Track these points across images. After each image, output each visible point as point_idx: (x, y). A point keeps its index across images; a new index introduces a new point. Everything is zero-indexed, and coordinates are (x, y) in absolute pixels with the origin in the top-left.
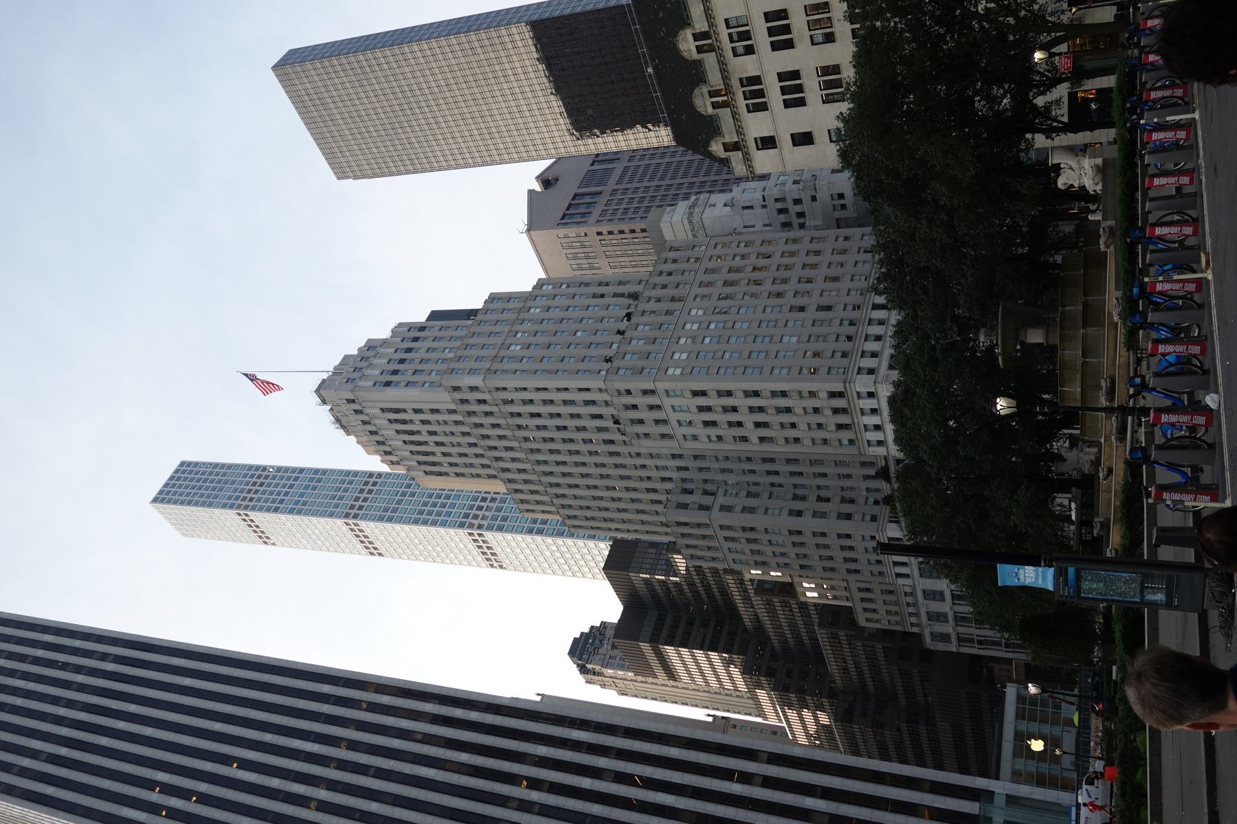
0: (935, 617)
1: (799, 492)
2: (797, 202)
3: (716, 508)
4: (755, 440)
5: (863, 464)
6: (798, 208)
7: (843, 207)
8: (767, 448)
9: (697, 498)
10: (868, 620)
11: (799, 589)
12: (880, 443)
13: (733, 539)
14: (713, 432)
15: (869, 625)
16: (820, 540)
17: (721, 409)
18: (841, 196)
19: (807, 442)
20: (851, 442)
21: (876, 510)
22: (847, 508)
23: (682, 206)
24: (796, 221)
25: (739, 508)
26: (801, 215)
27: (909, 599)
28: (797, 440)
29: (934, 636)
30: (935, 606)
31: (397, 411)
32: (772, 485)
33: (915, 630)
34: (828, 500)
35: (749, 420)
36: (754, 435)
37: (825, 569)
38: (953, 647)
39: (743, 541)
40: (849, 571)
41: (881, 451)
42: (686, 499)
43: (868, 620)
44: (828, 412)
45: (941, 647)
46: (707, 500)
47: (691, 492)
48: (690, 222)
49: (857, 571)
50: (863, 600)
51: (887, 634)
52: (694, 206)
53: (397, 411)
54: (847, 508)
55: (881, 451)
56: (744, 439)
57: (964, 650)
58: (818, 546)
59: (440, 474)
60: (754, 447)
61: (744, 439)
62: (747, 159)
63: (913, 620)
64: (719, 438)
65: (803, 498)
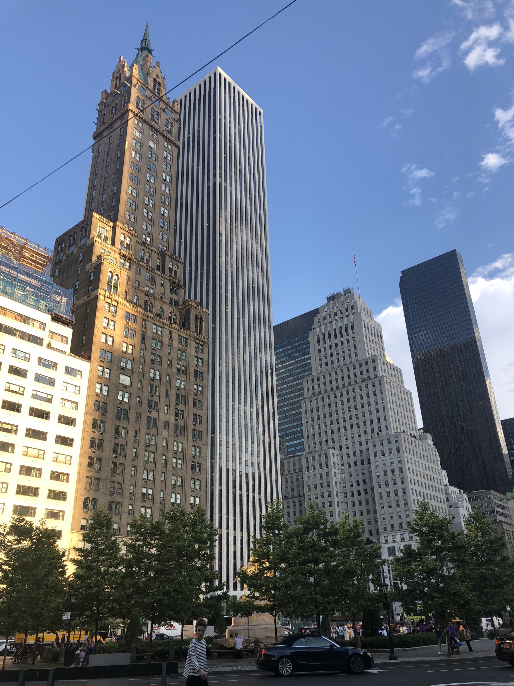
20: (385, 529)
31: (353, 328)
35: (391, 488)
39: (321, 481)
42: (336, 457)
44: (400, 521)
53: (353, 328)
59: (318, 341)
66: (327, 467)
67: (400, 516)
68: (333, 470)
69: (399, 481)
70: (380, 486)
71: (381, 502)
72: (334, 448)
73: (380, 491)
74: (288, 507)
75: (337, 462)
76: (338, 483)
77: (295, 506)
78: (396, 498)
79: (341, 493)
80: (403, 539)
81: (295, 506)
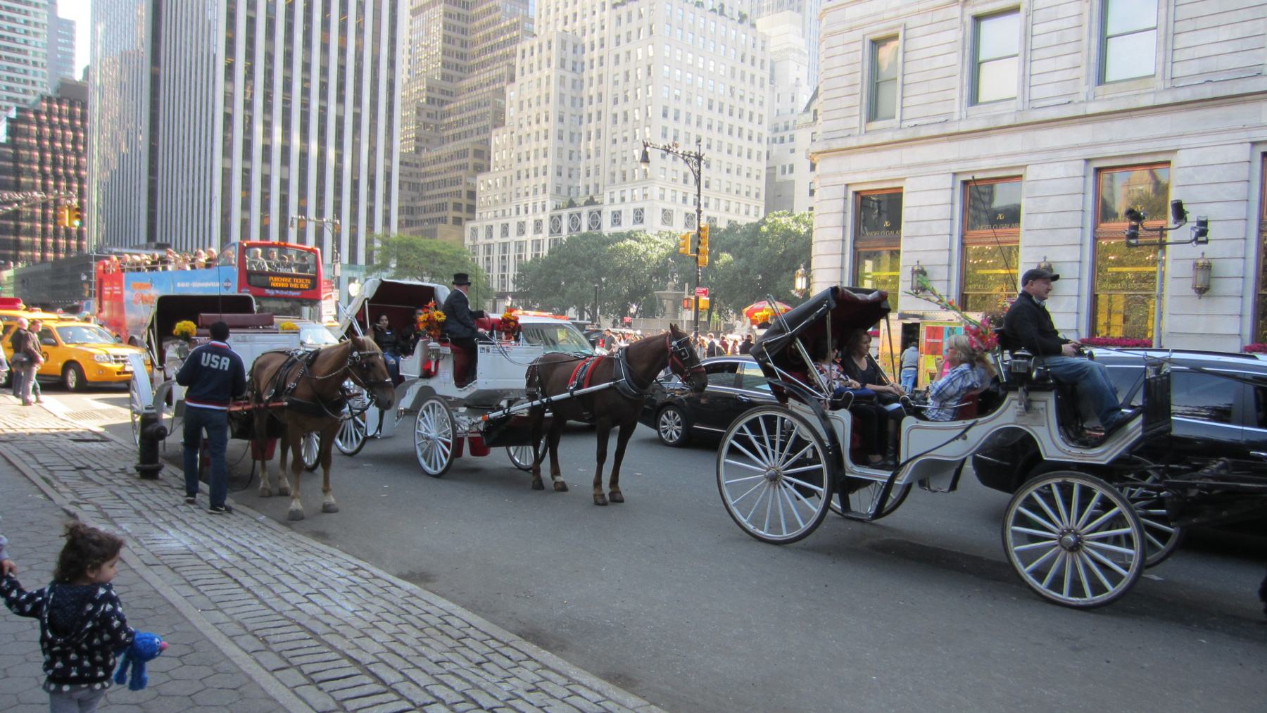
0: (489, 231)
1: (576, 136)
2: (792, 139)
3: (563, 72)
4: (615, 111)
5: (597, 186)
6: (787, 138)
7: (784, 172)
9: (570, 57)
11: (500, 130)
12: (612, 200)
13: (539, 85)
14: (621, 78)
18: (791, 170)
19: (613, 149)
21: (564, 191)
22: (565, 173)
23: (801, 43)
24: (778, 136)
25: (563, 91)
26: (782, 140)
27: (500, 213)
28: (615, 141)
29: (474, 230)
32: (581, 117)
33: (477, 215)
34: (570, 158)
40: (519, 172)
41: (607, 200)
42: (570, 49)
45: (468, 233)
46: (569, 65)
47: (574, 52)
48: (787, 49)
49: (519, 178)
51: (472, 195)
52: (800, 52)
54: (565, 173)
55: (607, 200)
56: (616, 102)
61: (616, 102)
62: (808, 125)
64: (616, 83)
65: (572, 140)
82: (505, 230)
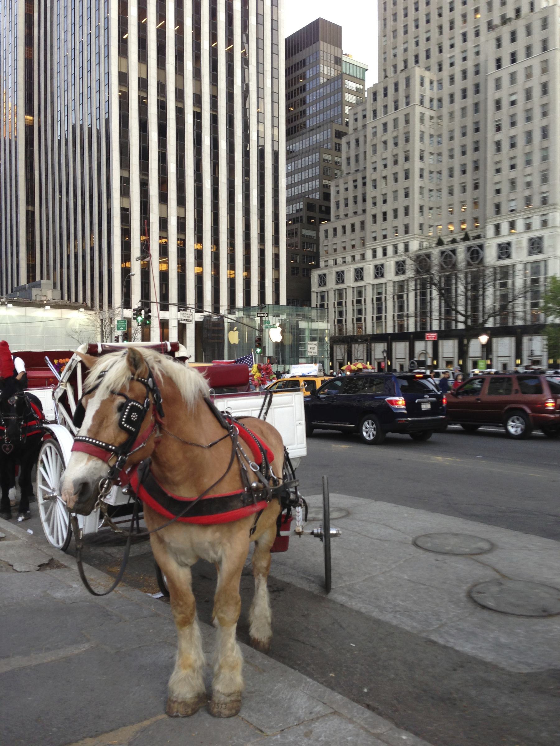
0: (340, 277)
8: (491, 148)
10: (326, 231)
15: (322, 234)
16: (401, 193)
17: (529, 107)
25: (423, 130)
30: (350, 276)
32: (440, 154)
33: (322, 264)
36: (503, 137)
37: (374, 198)
38: (315, 287)
39: (395, 134)
43: (326, 231)
50: (344, 227)
57: (314, 297)
58: (395, 192)
60: (492, 136)
63: (331, 262)
66: (408, 104)
67: (529, 184)
68: (418, 109)
69: (537, 113)
70: (498, 128)
71: (497, 159)
72: (428, 69)
73: (498, 136)
74: (347, 189)
75: (428, 94)
76: (427, 137)
77: (356, 187)
78: (528, 147)
79: (431, 154)
80: (528, 227)
81: (356, 187)
82: (359, 274)
